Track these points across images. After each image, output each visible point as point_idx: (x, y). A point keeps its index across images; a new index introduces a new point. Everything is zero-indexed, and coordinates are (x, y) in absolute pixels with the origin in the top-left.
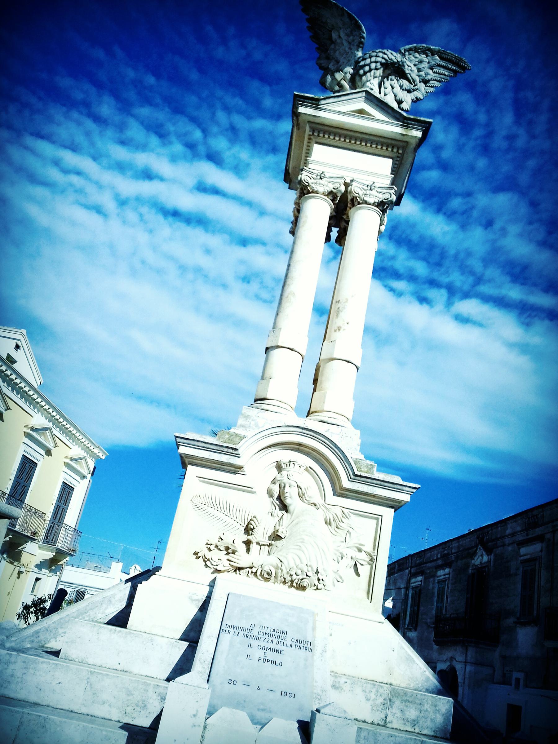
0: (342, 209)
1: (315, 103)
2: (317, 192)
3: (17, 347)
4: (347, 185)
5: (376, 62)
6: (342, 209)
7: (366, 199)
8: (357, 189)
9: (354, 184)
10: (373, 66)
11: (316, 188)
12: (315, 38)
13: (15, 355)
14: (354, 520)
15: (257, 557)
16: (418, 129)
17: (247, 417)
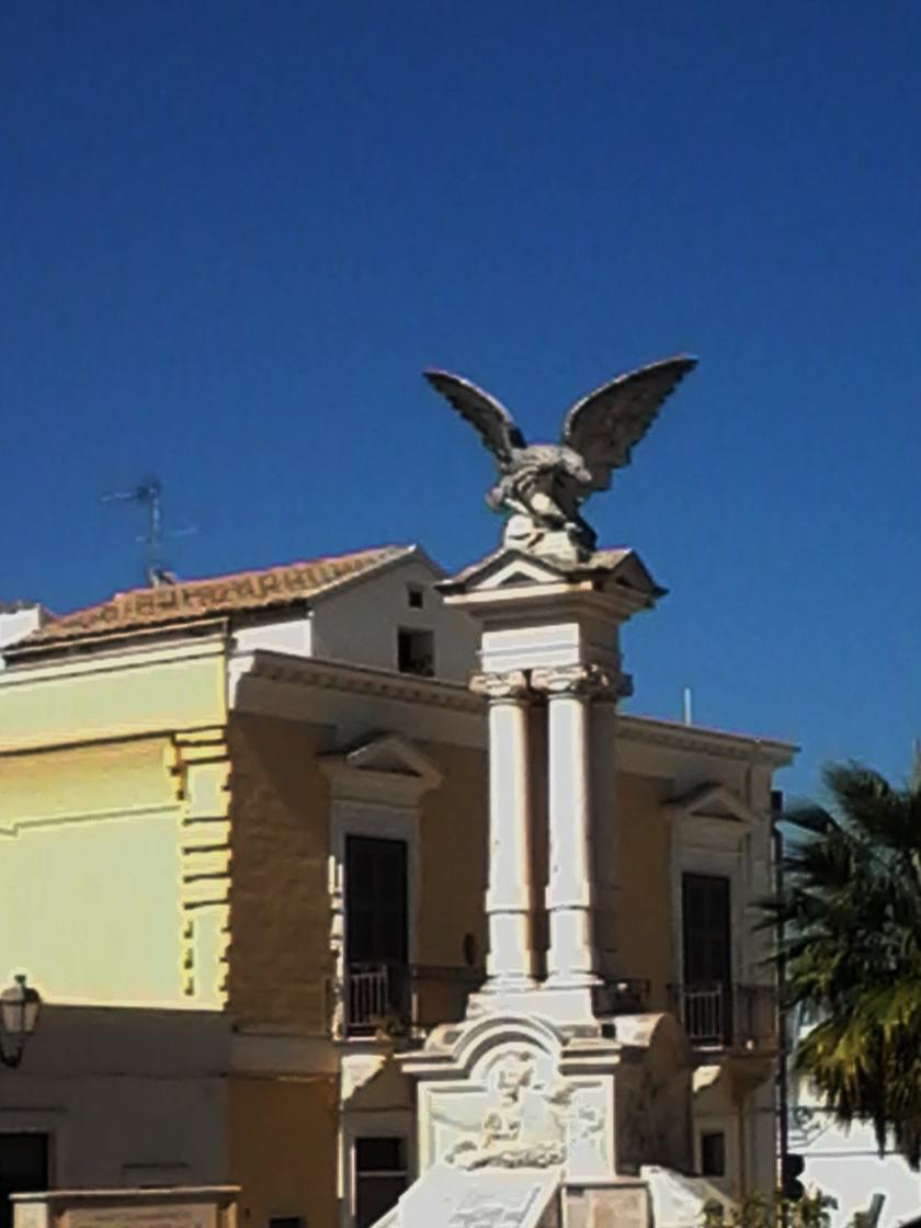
0: (534, 703)
1: (461, 588)
2: (494, 697)
3: (416, 599)
4: (527, 673)
5: (530, 473)
6: (534, 703)
7: (554, 687)
8: (538, 682)
9: (534, 674)
10: (529, 478)
11: (493, 692)
12: (466, 416)
13: (414, 619)
14: (580, 1091)
15: (498, 1148)
16: (586, 580)
17: (475, 1006)
